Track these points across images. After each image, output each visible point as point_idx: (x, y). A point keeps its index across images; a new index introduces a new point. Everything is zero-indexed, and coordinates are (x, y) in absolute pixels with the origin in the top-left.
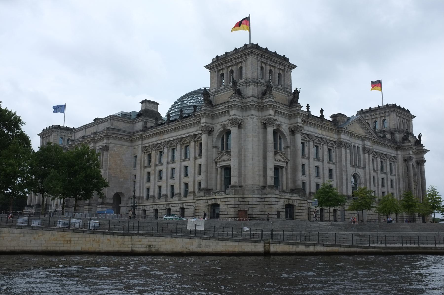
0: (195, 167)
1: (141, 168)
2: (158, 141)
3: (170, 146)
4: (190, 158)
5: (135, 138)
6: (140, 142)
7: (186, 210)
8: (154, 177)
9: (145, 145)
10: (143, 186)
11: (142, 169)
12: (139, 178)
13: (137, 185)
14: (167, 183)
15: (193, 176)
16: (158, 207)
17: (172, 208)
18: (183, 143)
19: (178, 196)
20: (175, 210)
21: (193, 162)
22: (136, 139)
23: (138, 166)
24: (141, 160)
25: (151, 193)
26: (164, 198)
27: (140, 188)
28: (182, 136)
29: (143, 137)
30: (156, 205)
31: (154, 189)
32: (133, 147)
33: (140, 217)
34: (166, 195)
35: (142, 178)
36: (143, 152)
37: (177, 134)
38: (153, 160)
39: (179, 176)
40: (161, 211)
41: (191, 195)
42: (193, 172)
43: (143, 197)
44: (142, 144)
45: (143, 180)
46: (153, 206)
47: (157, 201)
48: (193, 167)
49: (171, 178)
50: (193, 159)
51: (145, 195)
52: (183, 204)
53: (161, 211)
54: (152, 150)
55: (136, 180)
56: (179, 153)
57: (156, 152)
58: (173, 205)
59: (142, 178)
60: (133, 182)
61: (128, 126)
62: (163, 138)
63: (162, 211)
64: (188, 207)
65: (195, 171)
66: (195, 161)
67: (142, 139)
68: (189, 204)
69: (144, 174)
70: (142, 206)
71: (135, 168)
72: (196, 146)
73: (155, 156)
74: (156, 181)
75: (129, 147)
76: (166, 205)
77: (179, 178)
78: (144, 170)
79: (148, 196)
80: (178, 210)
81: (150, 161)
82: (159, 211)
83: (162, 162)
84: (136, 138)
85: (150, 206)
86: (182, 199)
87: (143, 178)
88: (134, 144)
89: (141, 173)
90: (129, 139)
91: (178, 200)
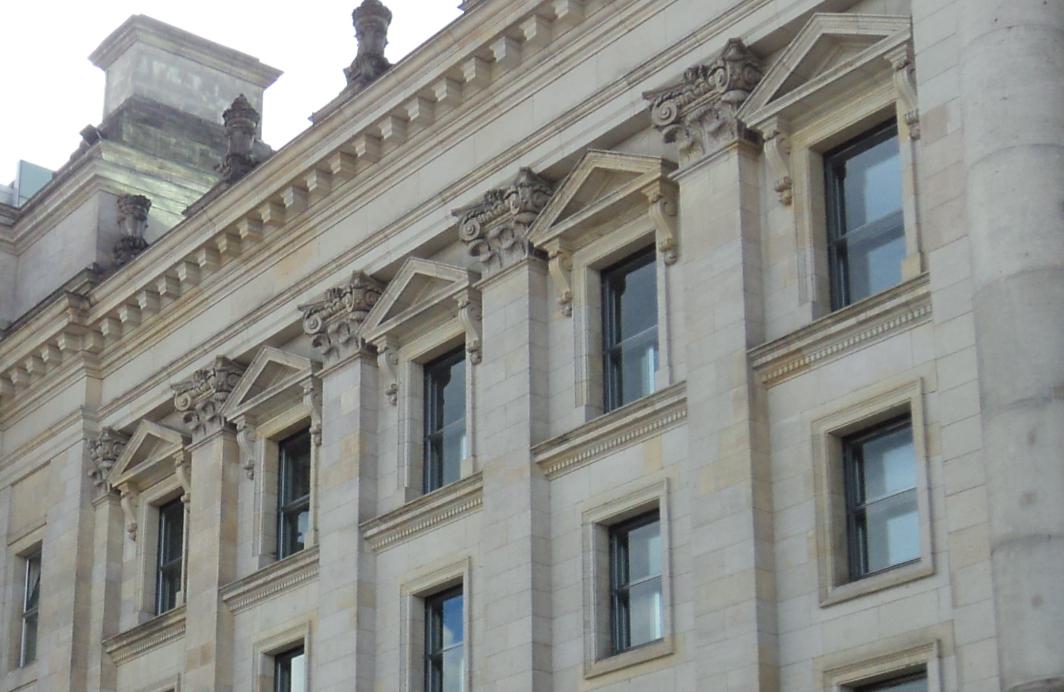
0: (763, 479)
2: (252, 317)
3: (392, 324)
4: (677, 387)
5: (20, 366)
6: (74, 393)
9: (120, 419)
11: (95, 668)
15: (750, 608)
18: (569, 223)
21: (744, 413)
22: (30, 365)
23: (55, 644)
24: (82, 577)
29: (105, 328)
36: (102, 493)
37: (496, 148)
38: (201, 542)
39: (524, 659)
42: (741, 555)
44: (89, 411)
48: (745, 488)
50: (740, 372)
54: (187, 440)
56: (522, 361)
57: (233, 454)
62: (307, 269)
65: (765, 533)
66: (759, 411)
67: (95, 355)
71: (29, 673)
72: (771, 197)
73: (229, 499)
81: (169, 574)
83: (307, 540)
84: (36, 355)
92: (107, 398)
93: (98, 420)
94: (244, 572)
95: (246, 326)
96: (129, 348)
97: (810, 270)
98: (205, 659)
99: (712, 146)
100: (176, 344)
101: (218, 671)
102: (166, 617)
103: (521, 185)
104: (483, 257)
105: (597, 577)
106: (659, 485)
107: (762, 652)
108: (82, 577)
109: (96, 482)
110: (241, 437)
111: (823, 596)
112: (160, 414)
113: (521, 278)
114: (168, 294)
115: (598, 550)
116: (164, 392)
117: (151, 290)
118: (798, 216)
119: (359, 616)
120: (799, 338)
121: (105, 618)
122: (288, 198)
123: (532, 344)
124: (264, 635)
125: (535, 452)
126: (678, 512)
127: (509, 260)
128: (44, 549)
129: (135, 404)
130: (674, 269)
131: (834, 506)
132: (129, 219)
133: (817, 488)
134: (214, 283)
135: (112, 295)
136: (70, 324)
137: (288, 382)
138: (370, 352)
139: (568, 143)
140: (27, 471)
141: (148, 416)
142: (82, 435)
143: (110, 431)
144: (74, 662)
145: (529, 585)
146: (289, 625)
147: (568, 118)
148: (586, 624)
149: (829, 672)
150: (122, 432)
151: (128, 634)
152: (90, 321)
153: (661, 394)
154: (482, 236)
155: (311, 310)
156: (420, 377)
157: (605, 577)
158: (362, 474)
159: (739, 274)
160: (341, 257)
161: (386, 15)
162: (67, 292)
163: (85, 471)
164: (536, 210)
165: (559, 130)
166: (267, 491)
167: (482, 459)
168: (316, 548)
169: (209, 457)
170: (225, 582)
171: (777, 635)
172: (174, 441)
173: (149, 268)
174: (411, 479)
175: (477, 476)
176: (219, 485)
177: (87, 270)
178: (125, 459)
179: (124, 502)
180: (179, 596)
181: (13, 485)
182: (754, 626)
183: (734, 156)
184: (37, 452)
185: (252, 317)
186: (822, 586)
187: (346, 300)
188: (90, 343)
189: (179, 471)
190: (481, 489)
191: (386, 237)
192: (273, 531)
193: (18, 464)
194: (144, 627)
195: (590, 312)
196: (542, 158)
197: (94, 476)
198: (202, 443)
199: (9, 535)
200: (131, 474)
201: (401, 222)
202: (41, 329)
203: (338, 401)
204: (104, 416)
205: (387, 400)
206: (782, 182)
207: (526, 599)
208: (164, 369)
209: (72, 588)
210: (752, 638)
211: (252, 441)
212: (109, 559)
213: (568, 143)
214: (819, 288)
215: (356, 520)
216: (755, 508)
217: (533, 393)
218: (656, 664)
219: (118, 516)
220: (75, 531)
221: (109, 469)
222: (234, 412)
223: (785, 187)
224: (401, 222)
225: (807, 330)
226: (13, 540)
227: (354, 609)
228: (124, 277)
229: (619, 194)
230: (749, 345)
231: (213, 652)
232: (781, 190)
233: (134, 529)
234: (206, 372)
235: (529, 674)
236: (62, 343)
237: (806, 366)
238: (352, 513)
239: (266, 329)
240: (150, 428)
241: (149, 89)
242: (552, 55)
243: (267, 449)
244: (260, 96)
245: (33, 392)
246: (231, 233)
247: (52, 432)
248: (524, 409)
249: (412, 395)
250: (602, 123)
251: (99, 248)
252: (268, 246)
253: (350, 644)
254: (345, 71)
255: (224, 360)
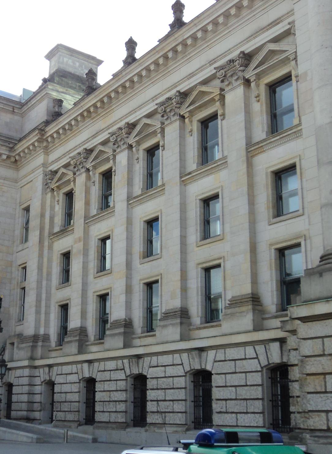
0: (251, 186)
1: (41, 242)
2: (94, 136)
3: (137, 138)
4: (225, 158)
5: (23, 151)
6: (40, 159)
7: (216, 380)
8: (83, 262)
9: (54, 167)
10: (48, 299)
11: (46, 244)
12: (35, 272)
13: (31, 299)
14: (129, 277)
15: (247, 225)
16: (95, 371)
17: (150, 373)
18: (191, 108)
19: (178, 321)
20: (163, 383)
21: (245, 166)
22: (26, 151)
23: (34, 236)
24: (42, 216)
25: (74, 323)
26: (120, 334)
27: (36, 306)
28: (187, 83)
29: (49, 139)
30: (90, 362)
31: (84, 303)
32: (20, 183)
33: (36, 406)
34: (128, 324)
35: (45, 274)
36: (49, 190)
39: (178, 241)
40: (107, 386)
41: (244, 309)
42: (244, 209)
43: (46, 338)
44: (44, 165)
45: (49, 279)
46: (79, 366)
47: (94, 348)
48: (245, 188)
49: (144, 258)
50: (244, 153)
51: (53, 331)
52: (204, 354)
53: (107, 386)
54: (75, 174)
55: (26, 284)
56: (177, 150)
57: (88, 178)
58: (154, 358)
59: (45, 274)
60: (19, 289)
61: (8, 120)
62: (111, 121)
63: (112, 386)
64: (228, 367)
65: (252, 202)
66: (250, 165)
67: (46, 148)
68: (232, 353)
69: (50, 261)
70: (41, 370)
71: (26, 245)
72: (253, 99)
73: (87, 192)
74: (91, 277)
75: (6, 182)
76: (126, 361)
77: (178, 248)
78: (50, 247)
79: (64, 330)
80: (181, 382)
81: (69, 215)
82: (99, 387)
83: (111, 204)
84: (28, 148)
85: (70, 367)
86: (197, 332)
87: (49, 274)
88: (23, 172)
89: (41, 256)
90: (8, 157)
91: (178, 337)
92: (50, 161)
93: (47, 168)
94: (92, 214)
95: (93, 139)
96: (57, 146)
97: (265, 122)
98: (80, 241)
99: (235, 84)
100: (71, 144)
101: (84, 244)
102: (68, 228)
103: (177, 96)
104: (165, 118)
105: (200, 216)
106: (219, 187)
107: (250, 239)
108: (42, 216)
109: (47, 187)
110: (91, 173)
111: (269, 222)
112: (66, 166)
113: (177, 124)
114: (69, 129)
115: (200, 208)
116: (67, 159)
117: (63, 128)
118: (261, 105)
119: (127, 228)
120: (262, 143)
121: (49, 228)
122: (106, 100)
123: (180, 144)
124: (98, 234)
125: (181, 177)
126: (225, 196)
127: (173, 119)
128: (30, 207)
129: (59, 163)
130: (223, 121)
131: (273, 194)
132: (57, 106)
133: (267, 188)
134: (83, 126)
135: (51, 129)
136: (38, 138)
137: (105, 156)
138: (130, 147)
139: (191, 83)
140: (26, 183)
141: (63, 166)
142: (42, 172)
143: (51, 171)
144: (40, 242)
145: (179, 218)
146: (106, 230)
147: (192, 75)
148: (197, 230)
149: (271, 245)
150: (55, 171)
151: (56, 233)
152: (45, 137)
153: (220, 160)
154: (165, 111)
155: (112, 134)
156: (146, 154)
157: (203, 216)
158: (128, 184)
159: (244, 123)
160: (121, 118)
161: (135, 44)
162: (38, 128)
163: (43, 183)
164: (181, 103)
165: (188, 79)
166: (99, 189)
167: (165, 180)
168: (114, 207)
169: (81, 179)
170: (86, 217)
171: (255, 233)
172: (71, 174)
173: (63, 121)
174: (143, 186)
175: (163, 185)
176: (84, 187)
177: (44, 122)
178: (55, 179)
179: (55, 193)
180: (72, 221)
181: (21, 187)
182: (248, 231)
183: (242, 87)
184: (28, 177)
185: (94, 136)
186: (269, 219)
187: (123, 131)
188: (45, 144)
189: (72, 183)
190: (164, 189)
191: (136, 112)
192: (101, 202)
193: (23, 181)
194: (61, 231)
195: (198, 134)
196: (183, 88)
197: (46, 185)
198: (79, 175)
199: (20, 203)
200: (57, 184)
201: (140, 107)
202: (30, 140)
203: (121, 162)
204: (49, 166)
205: (136, 161)
206: (257, 95)
207: (178, 222)
208: (68, 152)
209: (39, 219)
210: (247, 234)
211: (94, 174)
212: (51, 210)
213: (191, 83)
214: (268, 127)
215: (126, 198)
216: (249, 195)
217: (180, 159)
218: (218, 242)
219: (53, 197)
220: (40, 202)
221: (50, 183)
222: (89, 165)
223: (258, 96)
224: (140, 107)
225: (264, 140)
226: (21, 204)
227: (125, 226)
228: (55, 124)
229: (207, 98)
230: (247, 145)
231: (82, 239)
232: (256, 97)
233: (58, 201)
234: (80, 153)
235: (179, 245)
236: (36, 144)
237: (264, 151)
238: (124, 196)
239: (99, 140)
240: (63, 170)
241: (63, 67)
242: (186, 56)
243: (99, 177)
244: (97, 69)
245: (27, 159)
246: (88, 110)
247: (33, 171)
248: (178, 164)
249: (143, 160)
250: (202, 77)
251: (47, 115)
252: (99, 115)
253: (124, 236)
254: (123, 61)
255: (86, 149)
